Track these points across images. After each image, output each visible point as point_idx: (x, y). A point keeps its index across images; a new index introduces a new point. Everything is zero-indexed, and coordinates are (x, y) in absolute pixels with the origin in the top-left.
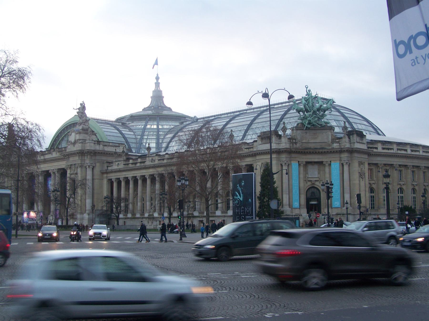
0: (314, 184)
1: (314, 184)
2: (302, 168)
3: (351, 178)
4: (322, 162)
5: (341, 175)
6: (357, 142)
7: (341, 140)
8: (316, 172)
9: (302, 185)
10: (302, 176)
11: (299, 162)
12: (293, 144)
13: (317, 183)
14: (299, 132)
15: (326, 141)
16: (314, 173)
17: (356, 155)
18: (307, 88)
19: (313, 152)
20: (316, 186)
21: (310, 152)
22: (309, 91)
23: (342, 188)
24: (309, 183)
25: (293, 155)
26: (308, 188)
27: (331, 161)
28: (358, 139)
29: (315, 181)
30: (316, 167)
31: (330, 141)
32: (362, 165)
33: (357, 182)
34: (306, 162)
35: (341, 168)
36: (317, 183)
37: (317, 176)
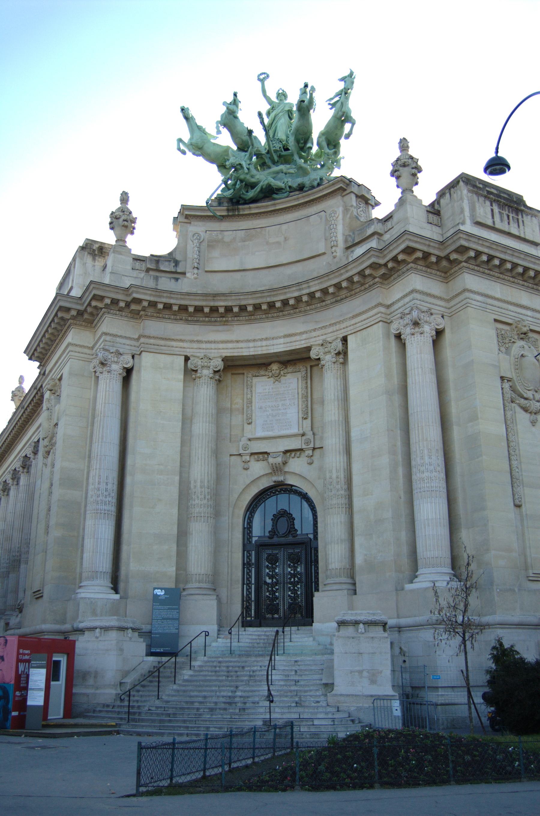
1: (276, 469)
2: (205, 391)
3: (454, 410)
4: (308, 349)
5: (397, 399)
6: (479, 224)
7: (389, 224)
9: (201, 471)
10: (202, 427)
11: (187, 359)
12: (156, 278)
17: (470, 280)
18: (262, 81)
19: (257, 307)
20: (291, 480)
21: (243, 308)
22: (282, 95)
23: (401, 471)
24: (258, 468)
25: (154, 327)
26: (254, 491)
27: (345, 340)
28: (484, 211)
29: (286, 452)
31: (341, 244)
32: (522, 343)
34: (225, 360)
35: (394, 360)
36: (296, 465)
37: (294, 430)
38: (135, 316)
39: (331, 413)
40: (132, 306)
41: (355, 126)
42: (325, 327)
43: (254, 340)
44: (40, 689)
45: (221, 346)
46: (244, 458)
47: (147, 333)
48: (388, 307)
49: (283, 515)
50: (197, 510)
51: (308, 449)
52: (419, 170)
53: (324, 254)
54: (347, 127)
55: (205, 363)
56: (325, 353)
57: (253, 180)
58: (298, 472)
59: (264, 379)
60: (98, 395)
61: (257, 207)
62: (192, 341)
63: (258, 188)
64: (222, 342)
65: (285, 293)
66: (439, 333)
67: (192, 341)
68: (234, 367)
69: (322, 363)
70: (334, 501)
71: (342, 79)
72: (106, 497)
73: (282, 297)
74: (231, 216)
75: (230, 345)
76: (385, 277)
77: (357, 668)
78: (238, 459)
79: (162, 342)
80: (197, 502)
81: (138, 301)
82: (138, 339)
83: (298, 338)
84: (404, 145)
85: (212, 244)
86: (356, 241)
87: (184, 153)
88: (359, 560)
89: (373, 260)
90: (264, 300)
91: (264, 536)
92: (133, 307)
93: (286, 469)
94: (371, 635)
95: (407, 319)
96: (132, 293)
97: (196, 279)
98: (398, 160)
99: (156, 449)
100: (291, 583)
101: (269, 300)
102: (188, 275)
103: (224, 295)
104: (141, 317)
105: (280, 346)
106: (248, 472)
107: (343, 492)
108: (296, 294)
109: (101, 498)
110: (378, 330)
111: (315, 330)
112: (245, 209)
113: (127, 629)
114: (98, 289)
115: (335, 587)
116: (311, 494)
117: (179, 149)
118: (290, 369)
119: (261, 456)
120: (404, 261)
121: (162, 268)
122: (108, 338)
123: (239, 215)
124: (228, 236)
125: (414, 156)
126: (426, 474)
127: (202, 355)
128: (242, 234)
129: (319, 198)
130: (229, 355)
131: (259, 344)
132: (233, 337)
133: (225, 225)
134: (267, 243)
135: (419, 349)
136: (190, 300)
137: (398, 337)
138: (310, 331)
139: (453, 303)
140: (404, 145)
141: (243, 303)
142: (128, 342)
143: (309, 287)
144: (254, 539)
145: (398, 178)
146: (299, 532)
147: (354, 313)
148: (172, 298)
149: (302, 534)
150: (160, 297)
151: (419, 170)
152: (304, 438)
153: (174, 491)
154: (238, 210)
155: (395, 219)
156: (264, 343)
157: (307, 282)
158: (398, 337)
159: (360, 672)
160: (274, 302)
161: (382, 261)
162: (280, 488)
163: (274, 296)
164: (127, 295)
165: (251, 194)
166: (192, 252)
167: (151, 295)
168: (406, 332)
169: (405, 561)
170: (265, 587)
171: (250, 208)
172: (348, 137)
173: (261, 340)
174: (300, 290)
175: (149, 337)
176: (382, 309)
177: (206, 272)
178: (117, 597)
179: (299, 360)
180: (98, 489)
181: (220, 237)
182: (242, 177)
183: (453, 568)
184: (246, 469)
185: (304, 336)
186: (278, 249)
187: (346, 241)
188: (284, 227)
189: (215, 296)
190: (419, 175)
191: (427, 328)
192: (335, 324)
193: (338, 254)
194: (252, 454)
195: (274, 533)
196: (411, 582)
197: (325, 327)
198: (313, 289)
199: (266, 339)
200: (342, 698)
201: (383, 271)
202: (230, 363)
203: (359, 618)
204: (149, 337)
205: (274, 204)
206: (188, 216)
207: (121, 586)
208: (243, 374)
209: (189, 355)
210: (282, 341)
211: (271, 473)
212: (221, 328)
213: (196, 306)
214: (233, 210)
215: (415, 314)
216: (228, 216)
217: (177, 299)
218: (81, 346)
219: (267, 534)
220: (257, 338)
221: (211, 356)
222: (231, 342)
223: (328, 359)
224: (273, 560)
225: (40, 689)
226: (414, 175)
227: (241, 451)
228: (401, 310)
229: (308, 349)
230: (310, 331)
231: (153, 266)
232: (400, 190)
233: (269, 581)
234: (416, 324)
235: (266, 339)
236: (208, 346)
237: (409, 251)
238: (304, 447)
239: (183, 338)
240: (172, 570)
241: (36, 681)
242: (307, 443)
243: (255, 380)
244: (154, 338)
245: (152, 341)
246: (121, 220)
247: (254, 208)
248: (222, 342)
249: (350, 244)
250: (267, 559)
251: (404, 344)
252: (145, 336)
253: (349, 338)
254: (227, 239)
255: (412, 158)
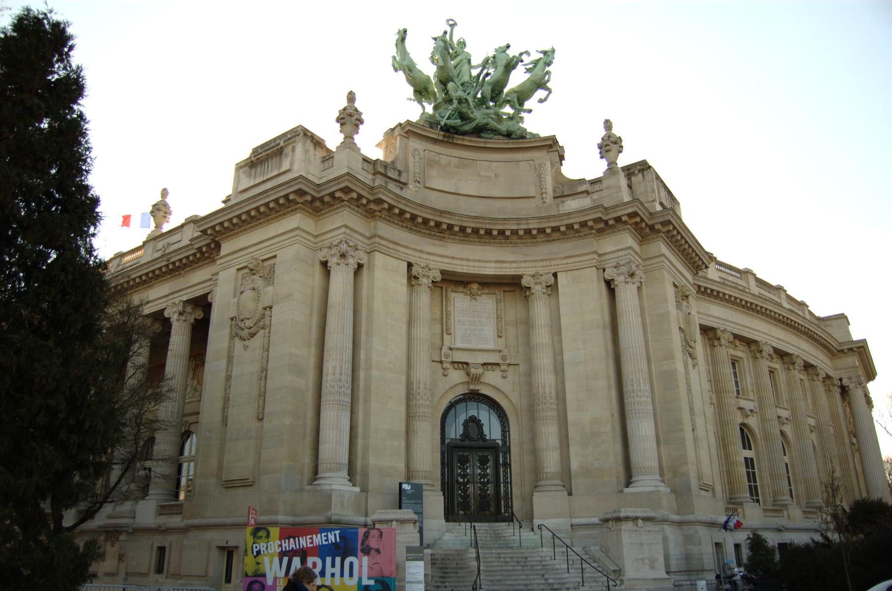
0: (477, 379)
1: (477, 379)
2: (424, 298)
4: (520, 277)
8: (489, 331)
10: (424, 332)
11: (410, 265)
13: (492, 377)
14: (415, 144)
15: (532, 191)
16: (476, 323)
19: (476, 231)
20: (484, 391)
24: (457, 376)
25: (385, 229)
27: (555, 275)
29: (485, 364)
30: (487, 303)
33: (680, 367)
34: (443, 272)
36: (492, 377)
37: (491, 346)
38: (368, 215)
39: (542, 336)
40: (315, 200)
41: (551, 95)
42: (535, 261)
43: (468, 260)
44: (419, 582)
45: (438, 259)
46: (502, 367)
47: (379, 233)
48: (600, 255)
49: (474, 422)
50: (422, 410)
51: (504, 364)
52: (362, 122)
53: (534, 197)
54: (540, 94)
55: (425, 272)
56: (536, 284)
57: (472, 116)
58: (493, 383)
59: (461, 295)
60: (637, 302)
61: (471, 141)
62: (415, 250)
63: (474, 124)
64: (440, 256)
65: (504, 224)
66: (360, 266)
67: (415, 250)
68: (453, 281)
69: (533, 291)
70: (549, 414)
71: (541, 52)
72: (341, 387)
73: (501, 227)
74: (447, 142)
75: (446, 260)
76: (600, 231)
77: (641, 556)
78: (439, 365)
79: (391, 245)
80: (421, 402)
81: (379, 201)
82: (372, 237)
83: (508, 265)
84: (351, 97)
85: (431, 163)
86: (566, 194)
87: (396, 70)
88: (574, 465)
89: (599, 215)
90: (484, 226)
91: (456, 439)
92: (372, 206)
93: (482, 380)
94: (647, 529)
95: (334, 251)
96: (379, 193)
97: (416, 191)
98: (345, 109)
99: (386, 347)
100: (481, 483)
101: (488, 227)
102: (411, 186)
103: (450, 213)
104: (375, 216)
105: (490, 270)
106: (447, 379)
107: (554, 406)
108: (514, 227)
109: (343, 389)
110: (592, 273)
111: (525, 261)
112: (458, 139)
113: (392, 521)
114: (350, 181)
115: (553, 488)
116: (504, 403)
117: (394, 66)
118: (486, 291)
119: (460, 365)
120: (339, 198)
121: (389, 175)
122: (348, 231)
123: (451, 143)
124: (444, 160)
125: (359, 109)
126: (643, 399)
127: (423, 265)
128: (455, 161)
129: (527, 148)
130: (444, 268)
131: (472, 264)
132: (448, 253)
133: (438, 148)
134: (479, 175)
135: (341, 279)
136: (421, 211)
137: (325, 264)
138: (521, 262)
139: (648, 263)
140: (351, 97)
141: (465, 224)
142: (361, 238)
143: (528, 224)
144: (447, 441)
145: (342, 125)
146: (488, 438)
147: (568, 255)
148: (406, 205)
149: (490, 440)
150: (399, 202)
151: (362, 122)
152: (501, 354)
153: (400, 391)
154: (453, 138)
155: (605, 183)
156: (476, 264)
157: (527, 219)
158: (325, 264)
159: (643, 560)
160: (491, 230)
161: (604, 218)
162: (474, 397)
163: (493, 224)
164: (370, 193)
165: (467, 127)
166: (413, 165)
167: (392, 199)
168: (333, 261)
169: (621, 469)
170: (456, 486)
171: (463, 139)
172: (541, 101)
173: (474, 261)
174: (518, 224)
175: (382, 238)
176: (596, 256)
177: (426, 187)
178: (357, 489)
179: (511, 285)
180: (340, 380)
181: (437, 158)
182: (464, 110)
183: (661, 475)
184: (445, 376)
185: (514, 265)
186: (466, 182)
187: (554, 191)
188: (494, 165)
189: (442, 212)
190: (361, 126)
191: (351, 261)
192: (546, 260)
193: (547, 201)
194: (453, 362)
195: (466, 435)
196: (627, 486)
197: (535, 261)
198: (531, 226)
199: (479, 261)
200: (634, 582)
201: (602, 225)
202: (446, 277)
203: (639, 514)
204: (382, 238)
205: (486, 142)
206: (407, 130)
207: (358, 478)
208: (442, 288)
209: (413, 262)
210: (493, 265)
211: (468, 382)
212: (437, 242)
213: (552, 228)
214: (449, 137)
215: (344, 247)
216: (443, 141)
217: (411, 207)
218: (307, 233)
219: (458, 437)
220: (471, 258)
221: (431, 266)
222: (448, 257)
223: (537, 289)
224: (464, 461)
225: (419, 582)
226: (357, 126)
227: (443, 359)
228: (331, 240)
229: (520, 277)
230: (521, 262)
231: (382, 170)
232: (342, 136)
233: (461, 480)
234: (343, 256)
235: (479, 261)
236: (428, 257)
237: (347, 190)
238: (501, 362)
239: (408, 245)
240: (402, 466)
241: (414, 574)
242: (504, 358)
243: (453, 295)
244: (386, 240)
245: (383, 242)
246: (354, 118)
247: (467, 141)
248: (440, 256)
249: (559, 195)
250: (459, 461)
251: (329, 271)
252: (379, 237)
253: (559, 275)
254: (442, 162)
255: (356, 110)
